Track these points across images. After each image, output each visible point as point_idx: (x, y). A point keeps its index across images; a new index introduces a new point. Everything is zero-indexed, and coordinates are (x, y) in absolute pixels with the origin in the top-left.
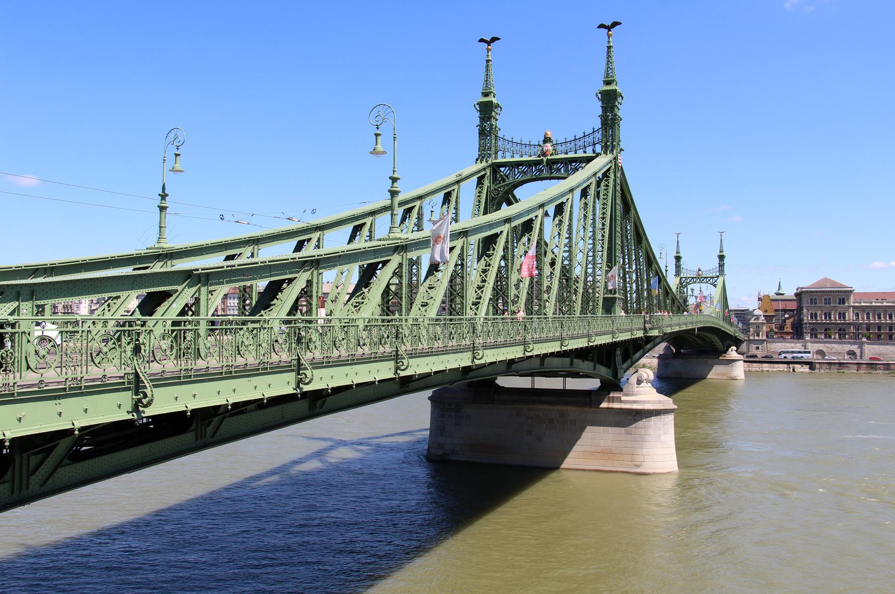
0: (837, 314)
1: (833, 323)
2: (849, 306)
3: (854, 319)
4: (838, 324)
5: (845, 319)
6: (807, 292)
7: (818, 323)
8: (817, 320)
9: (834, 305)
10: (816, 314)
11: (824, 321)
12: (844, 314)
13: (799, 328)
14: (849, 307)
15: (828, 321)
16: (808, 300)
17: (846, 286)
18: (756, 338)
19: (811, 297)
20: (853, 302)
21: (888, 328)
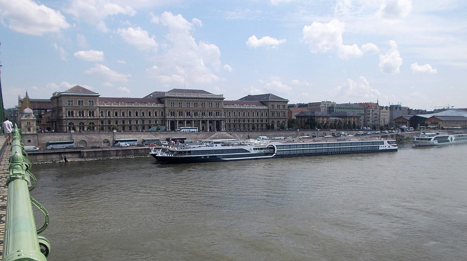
0: (88, 112)
1: (85, 119)
2: (96, 107)
3: (100, 116)
4: (89, 119)
5: (94, 115)
6: (65, 95)
7: (74, 119)
8: (73, 117)
9: (86, 106)
10: (72, 112)
11: (79, 118)
12: (93, 112)
13: (57, 122)
14: (97, 107)
15: (82, 118)
16: (66, 102)
17: (93, 92)
18: (28, 133)
19: (69, 99)
20: (99, 104)
21: (122, 122)
